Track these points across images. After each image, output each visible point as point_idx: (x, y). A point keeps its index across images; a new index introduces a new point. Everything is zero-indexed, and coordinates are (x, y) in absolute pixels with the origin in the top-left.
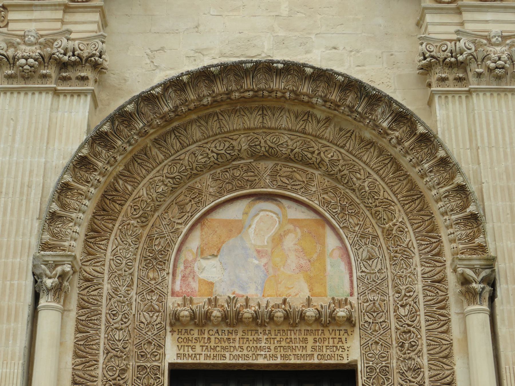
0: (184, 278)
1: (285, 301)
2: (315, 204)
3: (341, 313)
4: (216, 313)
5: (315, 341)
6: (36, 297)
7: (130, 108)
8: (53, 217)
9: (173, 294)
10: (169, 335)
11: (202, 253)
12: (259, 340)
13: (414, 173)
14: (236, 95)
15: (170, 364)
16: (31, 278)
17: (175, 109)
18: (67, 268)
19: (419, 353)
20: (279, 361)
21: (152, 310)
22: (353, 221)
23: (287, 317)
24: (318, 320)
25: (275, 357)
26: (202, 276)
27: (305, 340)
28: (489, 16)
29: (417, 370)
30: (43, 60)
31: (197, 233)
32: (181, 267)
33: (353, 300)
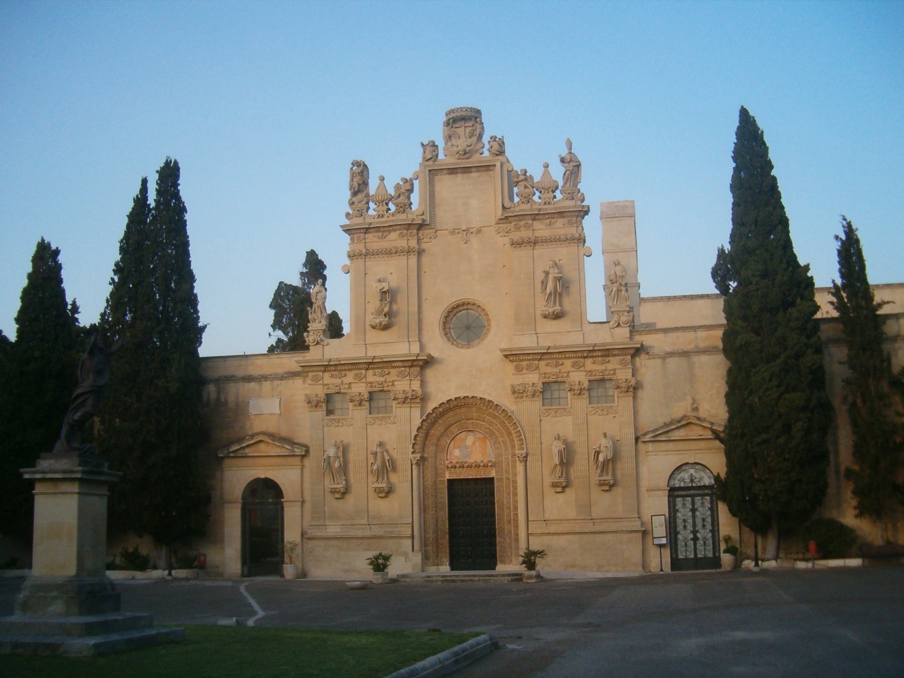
0: (450, 456)
1: (475, 462)
2: (484, 433)
3: (490, 464)
4: (458, 466)
5: (484, 471)
6: (412, 465)
7: (431, 412)
8: (414, 444)
9: (447, 460)
10: (446, 472)
11: (455, 448)
12: (469, 472)
13: (508, 425)
14: (460, 404)
15: (448, 479)
16: (410, 461)
17: (443, 410)
18: (419, 458)
19: (509, 475)
20: (474, 477)
21: (442, 465)
22: (494, 437)
23: (475, 466)
24: (484, 466)
25: (473, 476)
26: (455, 454)
27: (481, 471)
28: (531, 376)
29: (508, 479)
30: (406, 398)
31: (452, 442)
32: (449, 452)
33: (493, 460)
